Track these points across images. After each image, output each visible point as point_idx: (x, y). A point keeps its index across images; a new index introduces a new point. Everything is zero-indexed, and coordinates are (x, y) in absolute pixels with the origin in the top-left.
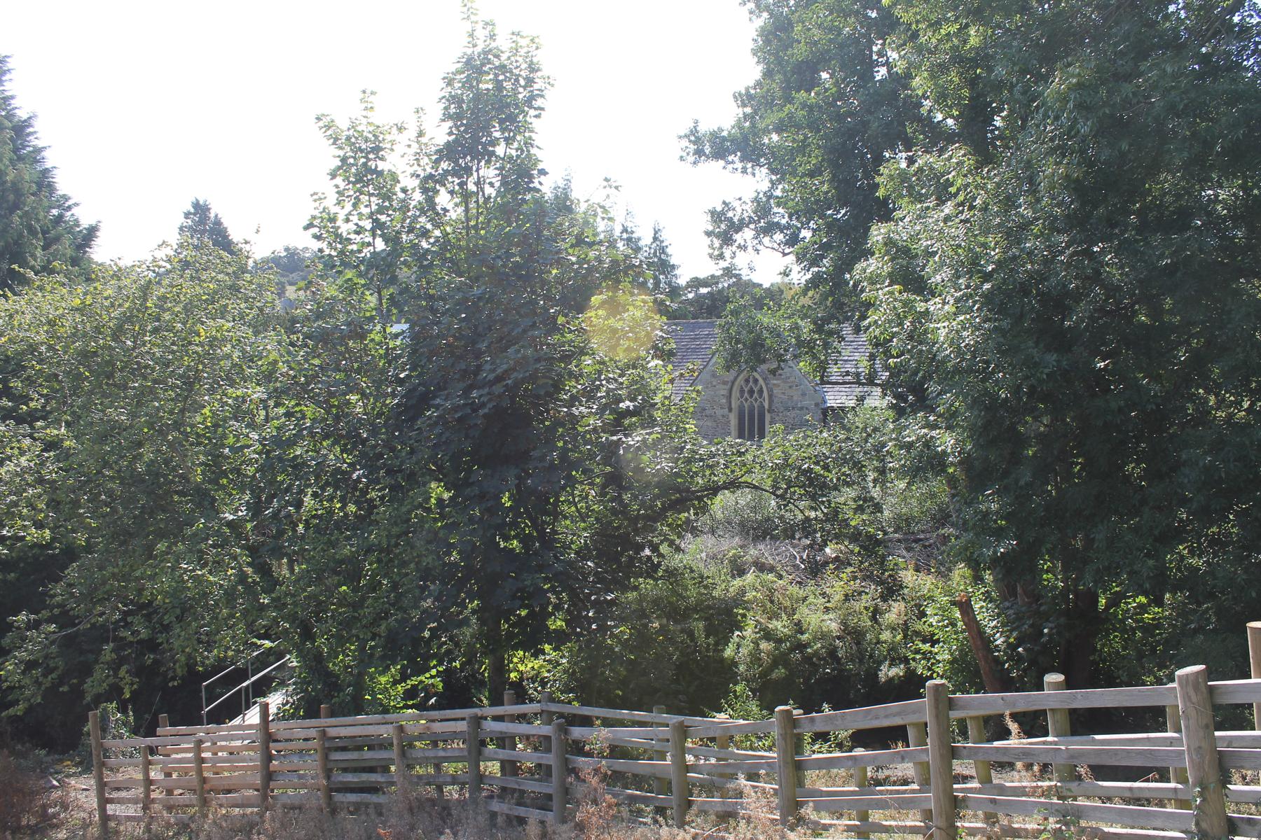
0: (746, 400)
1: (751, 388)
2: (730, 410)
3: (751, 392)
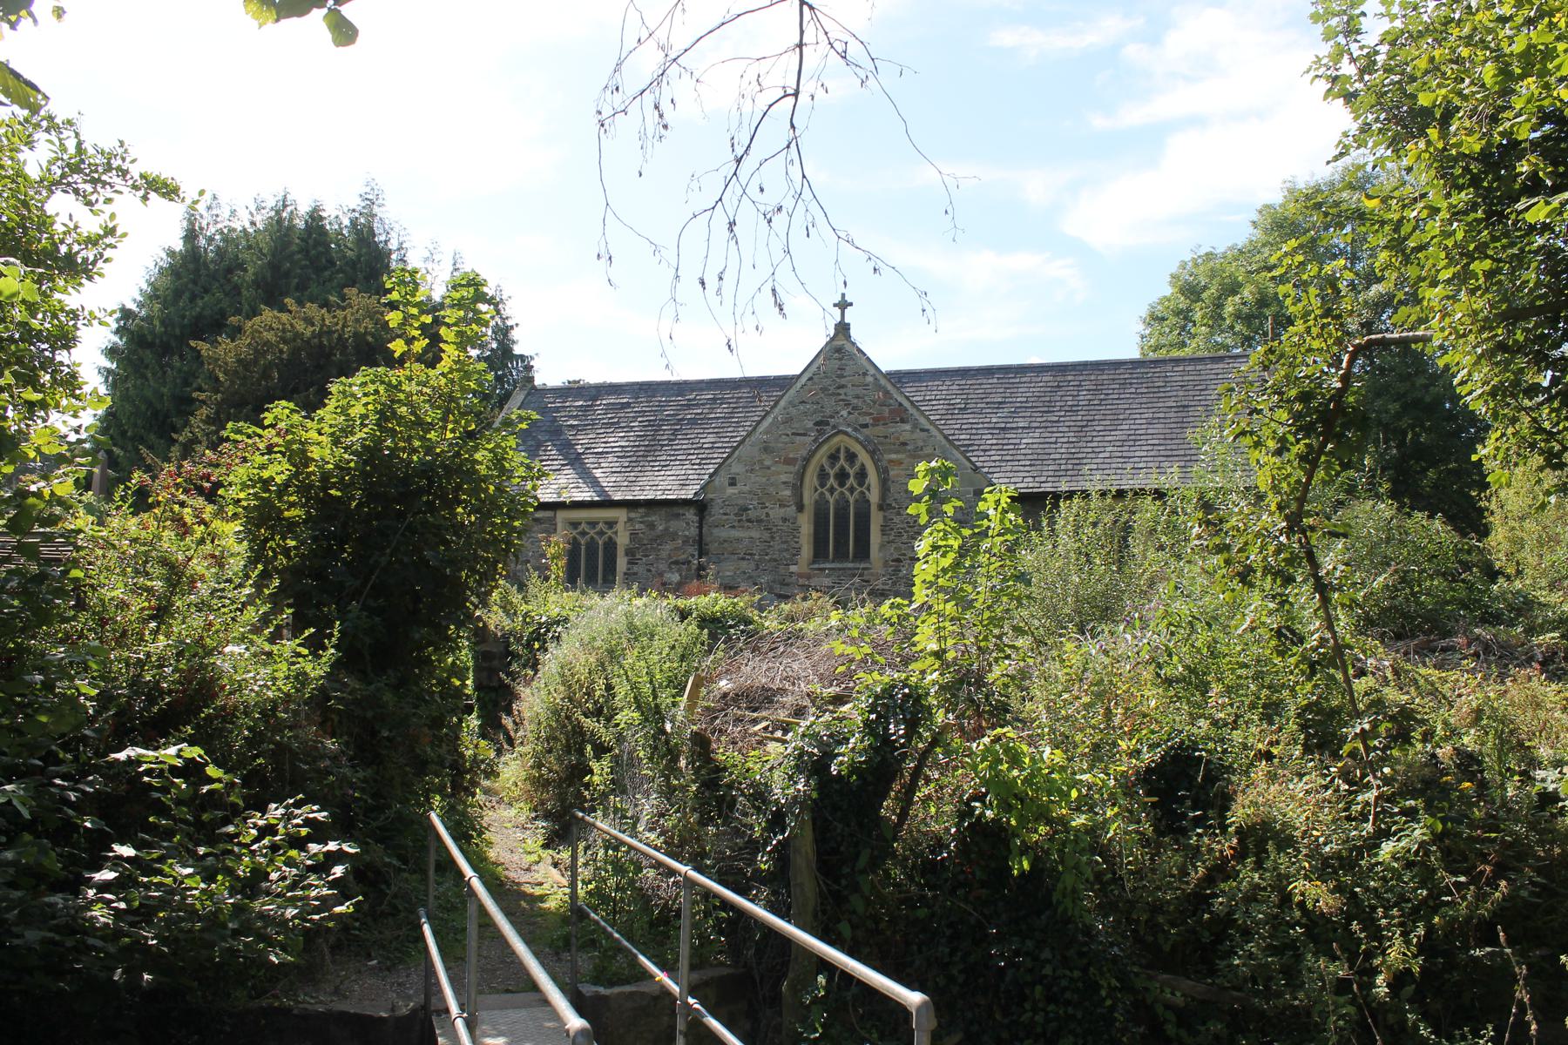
0: (832, 490)
1: (842, 469)
2: (800, 508)
3: (842, 476)
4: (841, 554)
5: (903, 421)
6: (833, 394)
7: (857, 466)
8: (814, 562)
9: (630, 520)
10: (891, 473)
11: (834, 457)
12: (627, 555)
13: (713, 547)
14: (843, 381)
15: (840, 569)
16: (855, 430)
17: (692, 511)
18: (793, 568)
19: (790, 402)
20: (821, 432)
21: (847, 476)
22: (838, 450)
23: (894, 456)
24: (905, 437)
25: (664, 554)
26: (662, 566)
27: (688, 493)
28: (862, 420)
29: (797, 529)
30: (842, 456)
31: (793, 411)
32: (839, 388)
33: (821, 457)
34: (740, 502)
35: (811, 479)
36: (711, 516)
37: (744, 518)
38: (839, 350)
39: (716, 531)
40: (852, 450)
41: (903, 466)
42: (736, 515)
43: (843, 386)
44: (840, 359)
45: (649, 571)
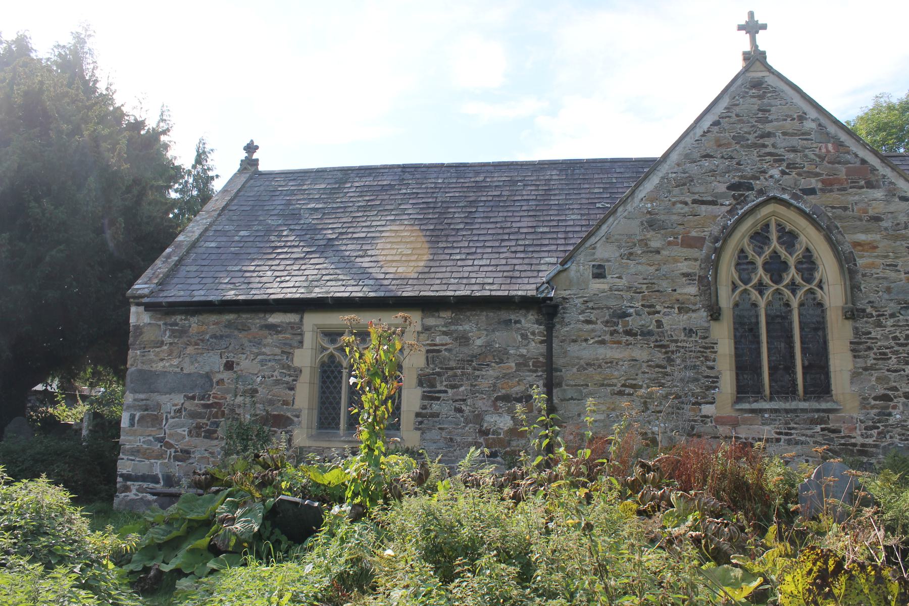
0: (761, 287)
1: (775, 255)
3: (776, 268)
4: (785, 390)
5: (870, 185)
6: (755, 145)
7: (799, 252)
8: (738, 400)
9: (426, 329)
10: (860, 262)
11: (760, 237)
12: (420, 384)
13: (569, 375)
14: (769, 128)
15: (787, 411)
16: (795, 196)
17: (532, 316)
18: (707, 409)
19: (687, 156)
20: (740, 200)
21: (785, 266)
22: (767, 226)
23: (861, 237)
24: (878, 208)
25: (484, 384)
26: (482, 404)
27: (526, 289)
28: (804, 183)
29: (711, 347)
30: (774, 235)
31: (693, 169)
32: (762, 136)
33: (741, 238)
34: (612, 303)
35: (727, 270)
36: (563, 323)
37: (620, 328)
38: (757, 84)
39: (574, 349)
40: (788, 227)
41: (878, 252)
42: (606, 323)
43: (769, 135)
44: (761, 97)
45: (460, 410)
